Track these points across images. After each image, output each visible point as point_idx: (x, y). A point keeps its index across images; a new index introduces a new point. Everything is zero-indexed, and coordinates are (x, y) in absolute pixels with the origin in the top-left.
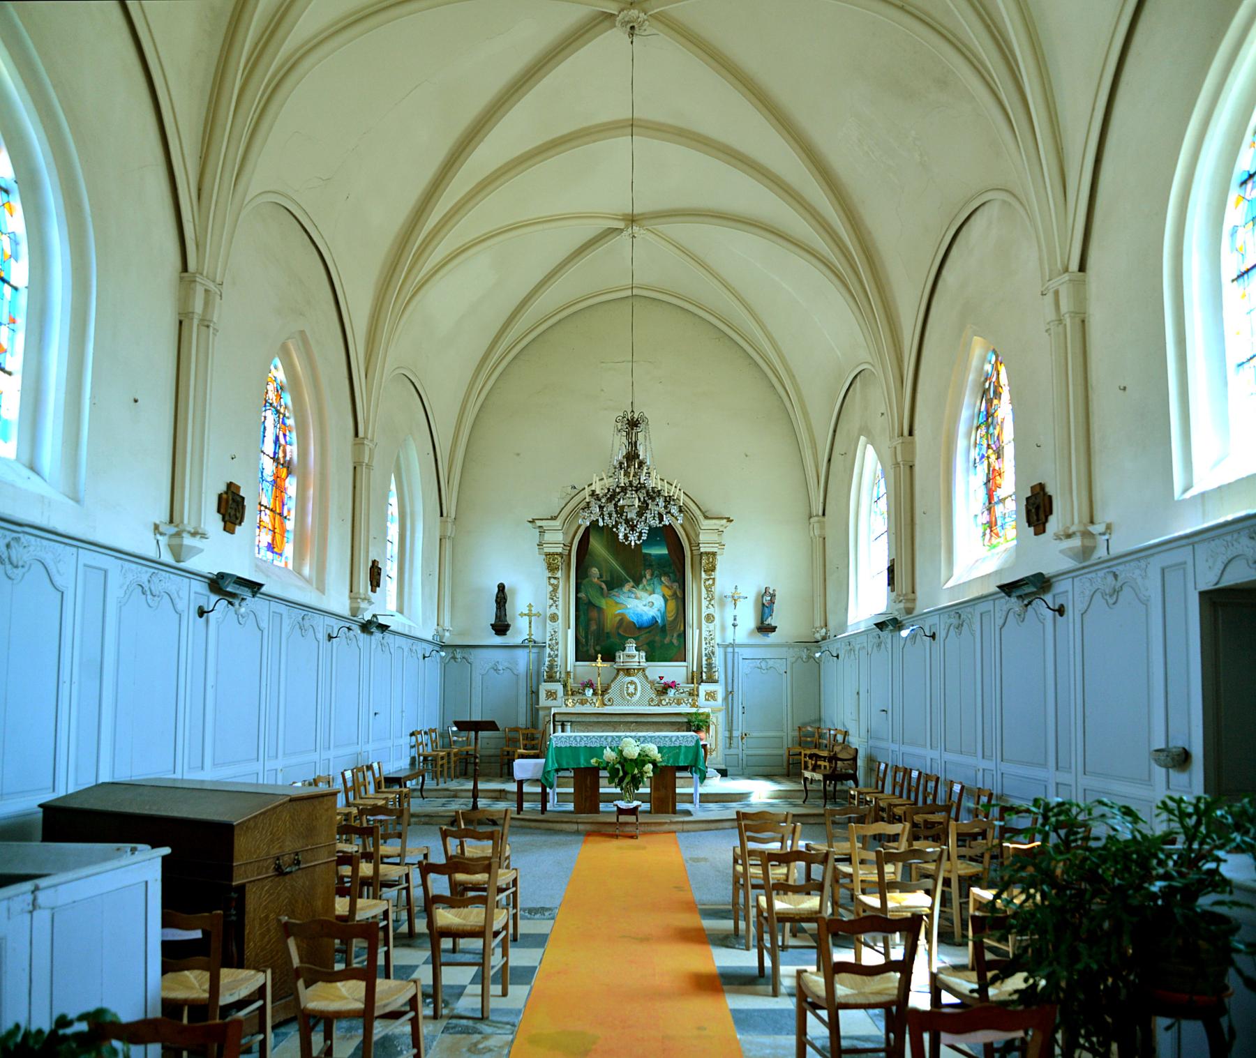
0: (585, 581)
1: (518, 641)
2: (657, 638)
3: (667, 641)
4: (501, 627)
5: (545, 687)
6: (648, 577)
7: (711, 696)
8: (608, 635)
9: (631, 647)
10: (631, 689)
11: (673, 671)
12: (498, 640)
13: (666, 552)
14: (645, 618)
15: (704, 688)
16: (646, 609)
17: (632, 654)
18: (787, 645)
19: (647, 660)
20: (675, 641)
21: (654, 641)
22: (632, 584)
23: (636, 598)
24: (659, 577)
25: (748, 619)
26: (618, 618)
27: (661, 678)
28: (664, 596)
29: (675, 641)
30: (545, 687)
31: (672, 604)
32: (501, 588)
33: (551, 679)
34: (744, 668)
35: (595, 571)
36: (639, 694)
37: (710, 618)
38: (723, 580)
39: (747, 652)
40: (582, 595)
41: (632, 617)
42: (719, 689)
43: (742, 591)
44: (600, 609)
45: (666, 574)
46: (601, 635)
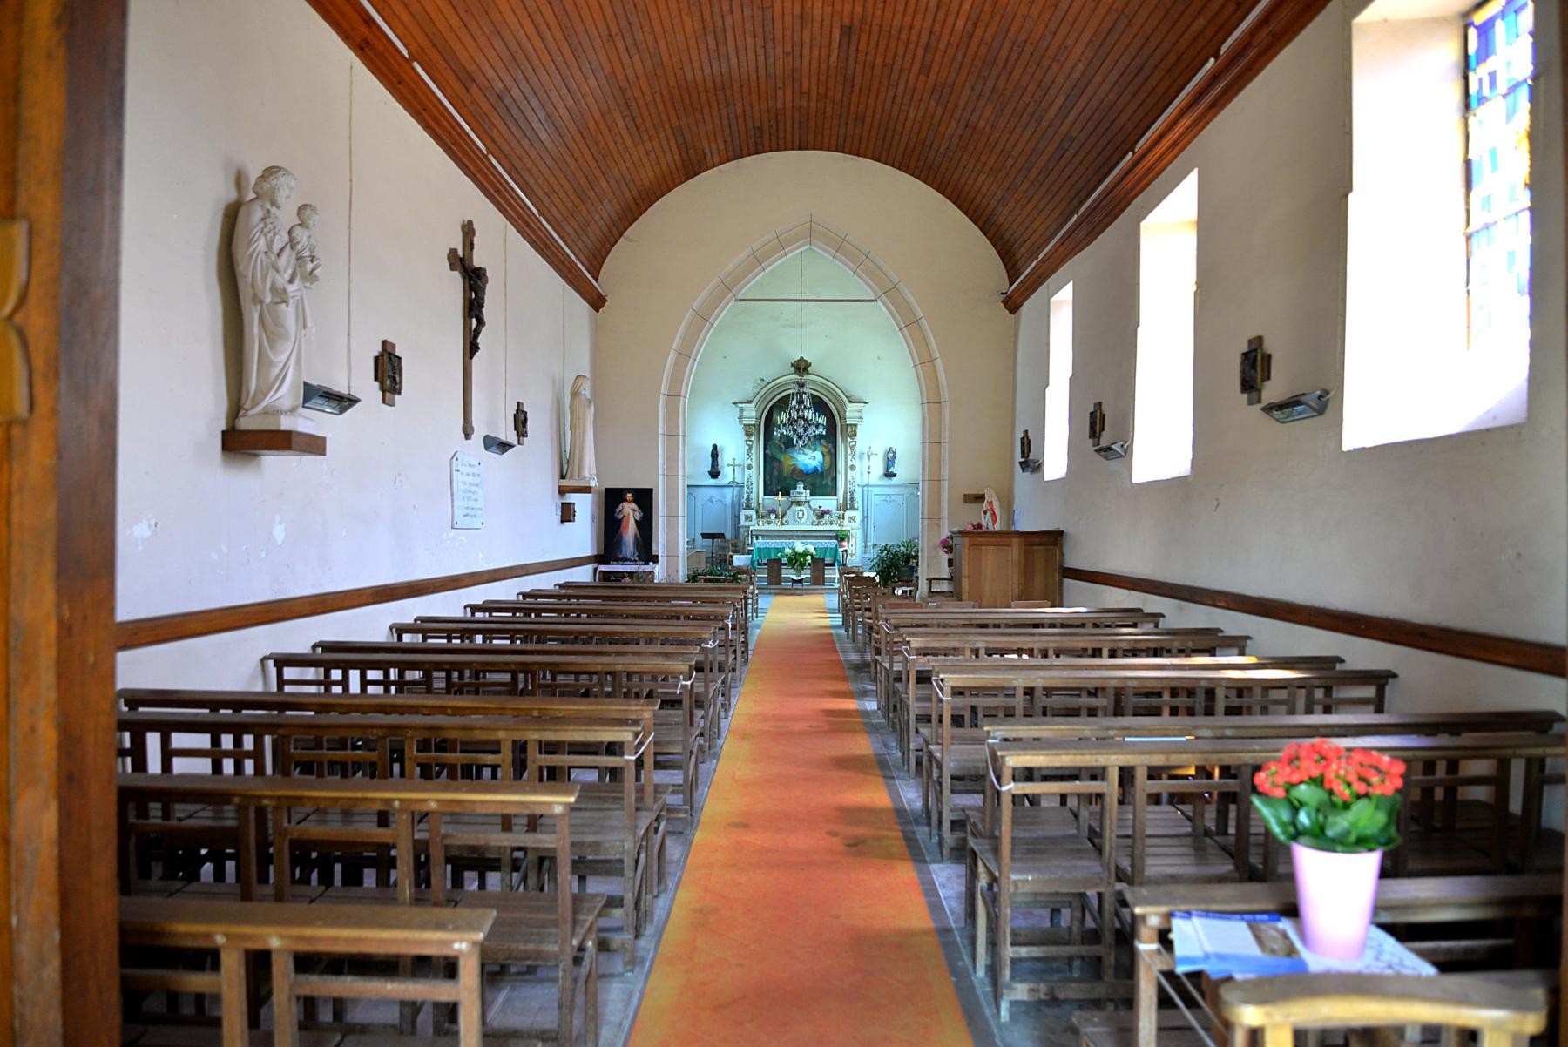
1: (726, 482)
4: (714, 474)
5: (744, 513)
7: (852, 519)
9: (800, 487)
11: (828, 503)
12: (713, 482)
15: (848, 514)
17: (801, 492)
18: (904, 486)
25: (878, 468)
31: (828, 458)
32: (715, 447)
33: (748, 507)
34: (875, 500)
37: (853, 468)
38: (863, 440)
39: (876, 490)
42: (858, 515)
43: (874, 450)
46: (780, 479)
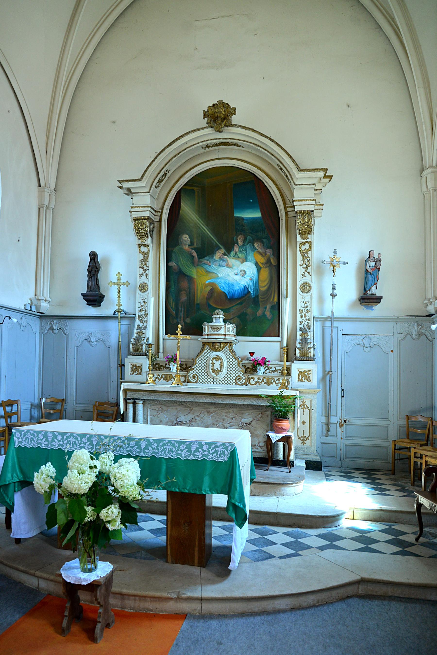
0: (176, 250)
1: (110, 312)
2: (249, 310)
3: (259, 313)
4: (94, 298)
5: (130, 361)
6: (240, 243)
7: (305, 375)
8: (198, 307)
9: (219, 319)
10: (217, 365)
11: (266, 347)
12: (92, 311)
13: (258, 215)
14: (237, 288)
15: (297, 367)
16: (237, 278)
17: (220, 327)
18: (395, 320)
19: (238, 334)
20: (268, 314)
21: (245, 314)
22: (223, 251)
23: (228, 266)
24: (252, 242)
25: (348, 288)
26: (209, 288)
27: (252, 354)
28: (257, 264)
29: (268, 314)
30: (130, 361)
31: (265, 273)
32: (93, 256)
33: (137, 352)
34: (344, 345)
35: (186, 238)
36: (225, 371)
37: (306, 287)
38: (321, 243)
39: (347, 328)
40: (173, 264)
41: (223, 287)
42: (314, 368)
43: (342, 256)
44: (190, 279)
45: (259, 240)
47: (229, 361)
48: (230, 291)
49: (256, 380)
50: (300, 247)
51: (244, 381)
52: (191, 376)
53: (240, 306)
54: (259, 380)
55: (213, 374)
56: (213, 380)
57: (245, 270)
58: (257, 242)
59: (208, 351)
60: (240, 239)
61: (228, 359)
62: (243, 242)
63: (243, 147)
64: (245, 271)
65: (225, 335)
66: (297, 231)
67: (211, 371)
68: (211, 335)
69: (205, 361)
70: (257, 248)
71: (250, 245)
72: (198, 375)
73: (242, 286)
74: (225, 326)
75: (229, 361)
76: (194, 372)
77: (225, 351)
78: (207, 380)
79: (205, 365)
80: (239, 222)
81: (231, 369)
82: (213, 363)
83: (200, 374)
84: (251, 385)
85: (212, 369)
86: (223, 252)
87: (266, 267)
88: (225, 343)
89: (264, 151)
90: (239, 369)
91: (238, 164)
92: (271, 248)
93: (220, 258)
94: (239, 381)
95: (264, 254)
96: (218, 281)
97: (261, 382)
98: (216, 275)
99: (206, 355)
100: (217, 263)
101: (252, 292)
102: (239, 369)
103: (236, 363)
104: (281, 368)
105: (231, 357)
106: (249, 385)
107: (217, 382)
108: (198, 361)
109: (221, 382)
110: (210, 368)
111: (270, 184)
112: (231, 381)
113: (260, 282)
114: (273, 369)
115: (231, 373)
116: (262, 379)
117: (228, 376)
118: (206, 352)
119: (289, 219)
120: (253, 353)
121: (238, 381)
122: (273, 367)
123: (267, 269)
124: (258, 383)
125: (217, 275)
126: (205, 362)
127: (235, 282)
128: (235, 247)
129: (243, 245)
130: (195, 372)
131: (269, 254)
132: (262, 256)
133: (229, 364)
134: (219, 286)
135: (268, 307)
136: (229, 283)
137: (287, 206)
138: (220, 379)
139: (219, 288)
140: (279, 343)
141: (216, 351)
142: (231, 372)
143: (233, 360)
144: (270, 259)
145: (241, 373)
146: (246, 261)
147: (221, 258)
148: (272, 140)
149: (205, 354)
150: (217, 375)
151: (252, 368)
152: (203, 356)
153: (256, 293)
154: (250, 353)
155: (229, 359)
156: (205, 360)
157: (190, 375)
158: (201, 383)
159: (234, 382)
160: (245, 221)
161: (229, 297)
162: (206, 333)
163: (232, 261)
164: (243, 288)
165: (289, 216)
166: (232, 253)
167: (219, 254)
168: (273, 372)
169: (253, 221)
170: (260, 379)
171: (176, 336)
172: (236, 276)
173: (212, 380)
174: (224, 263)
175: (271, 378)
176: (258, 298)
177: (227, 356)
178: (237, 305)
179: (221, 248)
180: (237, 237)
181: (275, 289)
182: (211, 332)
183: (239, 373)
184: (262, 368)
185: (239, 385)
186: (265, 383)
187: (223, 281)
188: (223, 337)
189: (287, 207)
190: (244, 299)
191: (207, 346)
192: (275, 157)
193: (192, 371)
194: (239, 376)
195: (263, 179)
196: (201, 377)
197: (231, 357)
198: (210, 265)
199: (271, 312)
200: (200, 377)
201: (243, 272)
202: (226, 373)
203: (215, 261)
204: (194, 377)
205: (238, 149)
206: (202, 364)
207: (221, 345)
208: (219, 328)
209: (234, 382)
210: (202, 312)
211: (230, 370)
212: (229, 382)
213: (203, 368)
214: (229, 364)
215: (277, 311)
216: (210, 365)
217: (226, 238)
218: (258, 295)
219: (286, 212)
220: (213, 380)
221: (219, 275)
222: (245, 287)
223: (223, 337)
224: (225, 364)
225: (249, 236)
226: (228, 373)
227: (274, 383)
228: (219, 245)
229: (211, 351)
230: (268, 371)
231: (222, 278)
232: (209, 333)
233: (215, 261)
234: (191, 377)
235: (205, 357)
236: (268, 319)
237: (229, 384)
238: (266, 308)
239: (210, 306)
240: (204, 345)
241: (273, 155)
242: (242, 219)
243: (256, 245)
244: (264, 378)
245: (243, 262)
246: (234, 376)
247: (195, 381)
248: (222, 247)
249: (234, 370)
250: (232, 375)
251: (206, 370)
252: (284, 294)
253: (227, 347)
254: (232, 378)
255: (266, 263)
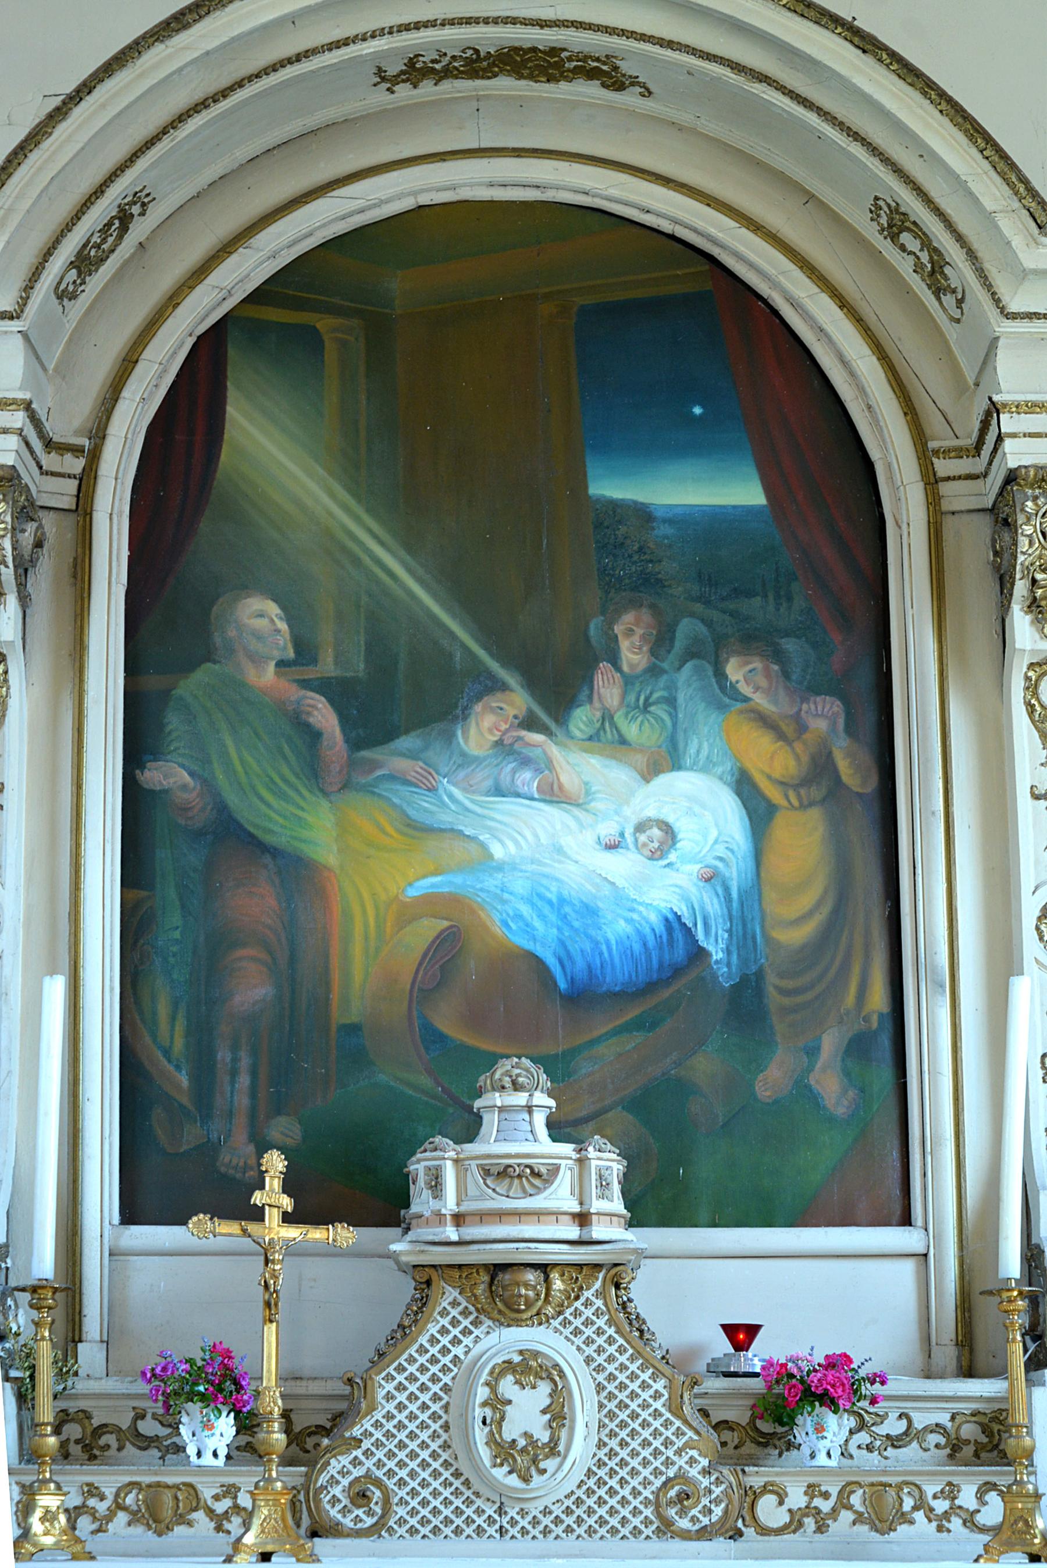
0: (192, 686)
2: (706, 1066)
3: (772, 1079)
6: (633, 655)
8: (354, 1046)
9: (519, 1117)
10: (526, 1411)
13: (743, 491)
14: (617, 928)
16: (623, 867)
19: (645, 1206)
20: (830, 1086)
21: (680, 1089)
22: (518, 700)
23: (553, 794)
24: (710, 655)
26: (429, 928)
27: (741, 1335)
28: (744, 787)
29: (830, 1086)
31: (804, 840)
35: (259, 619)
36: (581, 1447)
40: (167, 775)
41: (519, 921)
44: (297, 873)
45: (755, 640)
46: (306, 1041)
47: (611, 1387)
48: (574, 948)
49: (797, 1498)
50: (1032, 688)
51: (718, 1511)
52: (337, 1491)
53: (639, 1037)
54: (818, 1502)
55: (499, 1473)
56: (501, 1511)
57: (671, 819)
58: (739, 653)
59: (455, 1322)
60: (629, 633)
61: (599, 1369)
62: (653, 653)
63: (648, 93)
64: (669, 831)
65: (582, 1219)
66: (1021, 588)
67: (485, 1453)
68: (483, 1217)
69: (436, 1388)
70: (745, 689)
71: (697, 670)
72: (390, 1484)
73: (654, 918)
74: (582, 1162)
75: (611, 1387)
76: (356, 1462)
77: (578, 1322)
78: (458, 1512)
79: (435, 1417)
80: (623, 530)
81: (623, 1434)
82: (498, 1403)
83: (403, 1473)
84: (764, 1531)
85: (492, 1441)
86: (522, 712)
87: (803, 807)
88: (580, 1266)
89: (799, 111)
90: (679, 1433)
91: (614, 192)
92: (829, 692)
93: (499, 743)
94: (682, 1512)
95: (789, 729)
96: (491, 882)
97: (834, 1512)
98: (473, 847)
99: (445, 1351)
100: (483, 777)
101: (717, 954)
102: (679, 1433)
103: (657, 1395)
104: (944, 1418)
105: (623, 1359)
106: (749, 1532)
107: (524, 1523)
108: (390, 1387)
109: (557, 1521)
110: (480, 1435)
111: (823, 319)
112: (625, 1512)
113: (770, 896)
114: (894, 1427)
115: (623, 1463)
116: (834, 1491)
117: (601, 1483)
118: (444, 1331)
119: (950, 525)
120: (752, 1330)
121: (672, 1512)
122: (893, 1416)
123: (815, 815)
124: (810, 1523)
125: (483, 846)
126: (436, 1398)
127: (607, 890)
128: (599, 679)
129: (653, 671)
130: (369, 1464)
131: (819, 725)
132: (781, 736)
133: (611, 1406)
134: (497, 917)
135: (831, 1042)
136: (562, 901)
137: (932, 445)
138: (547, 1501)
139: (498, 929)
140: (908, 1268)
141: (518, 1323)
142: (623, 1454)
143: (633, 1377)
144: (830, 754)
145: (692, 1461)
146: (676, 765)
147: (503, 748)
148: (866, 43)
149: (433, 1341)
150: (526, 1479)
151: (752, 1422)
152: (422, 1360)
153: (744, 962)
154: (730, 1330)
155: (611, 1368)
156: (434, 1379)
157: (333, 1481)
158: (413, 1531)
159: (647, 1522)
160: (664, 530)
161: (562, 985)
162: (450, 1203)
163: (576, 764)
164: (660, 928)
165: (945, 506)
166: (582, 719)
167: (488, 720)
168: (895, 1442)
169: (713, 528)
170: (826, 1495)
171: (252, 1227)
172: (609, 856)
173: (490, 1511)
174: (526, 775)
175: (899, 1487)
176: (759, 992)
177: (590, 1351)
178: (618, 1031)
179: (504, 687)
180: (610, 624)
181: (867, 934)
182: (482, 1197)
183: (681, 1462)
184: (831, 1420)
185: (685, 1535)
186: (859, 1519)
187: (520, 886)
188: (573, 1232)
189: (936, 452)
190: (666, 993)
191: (453, 1293)
192: (875, 151)
193: (345, 1460)
194: (681, 1477)
195: (776, 285)
196: (413, 1493)
197: (623, 1359)
198: (432, 789)
199: (847, 1073)
200: (402, 1493)
201: (656, 832)
202: (591, 1463)
203: (466, 760)
204: (360, 1497)
205: (610, 108)
206: (413, 1407)
207: (547, 1279)
208: (539, 1176)
209: (647, 1522)
210: (382, 1078)
211: (613, 1443)
212: (614, 1522)
213: (424, 1436)
214: (611, 1406)
215: (886, 1074)
216: (479, 1413)
217: (550, 621)
218: (760, 975)
219: (931, 481)
220: (501, 1511)
221: (498, 851)
222: (675, 927)
223: (573, 1232)
224: (585, 1413)
225: (692, 615)
226: (600, 1464)
227: (919, 1516)
228: (494, 666)
229: (476, 1323)
230: (863, 1438)
231: (514, 867)
232: (467, 1207)
233: (466, 760)
234: (335, 1500)
235: (434, 1360)
236: (831, 1119)
237: (614, 1531)
238: (813, 1051)
239: (433, 1038)
240: (428, 1283)
241: (856, 136)
242: (644, 514)
243: (735, 671)
244: (845, 1492)
245: (651, 771)
246: (646, 1483)
247: (369, 1521)
248: (511, 679)
249: (645, 1443)
250: (634, 1472)
251: (445, 1446)
252: (934, 970)
253: (588, 1294)
254: (635, 1493)
255: (806, 782)
